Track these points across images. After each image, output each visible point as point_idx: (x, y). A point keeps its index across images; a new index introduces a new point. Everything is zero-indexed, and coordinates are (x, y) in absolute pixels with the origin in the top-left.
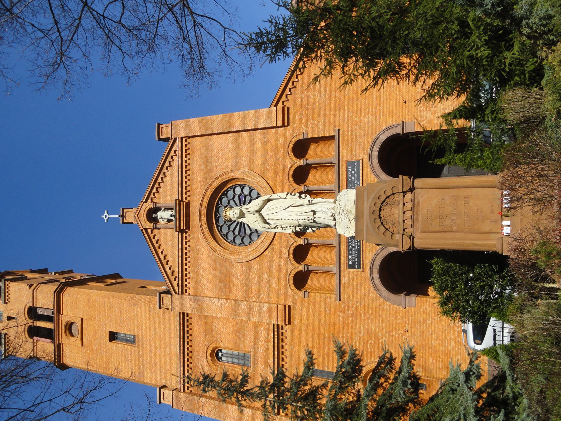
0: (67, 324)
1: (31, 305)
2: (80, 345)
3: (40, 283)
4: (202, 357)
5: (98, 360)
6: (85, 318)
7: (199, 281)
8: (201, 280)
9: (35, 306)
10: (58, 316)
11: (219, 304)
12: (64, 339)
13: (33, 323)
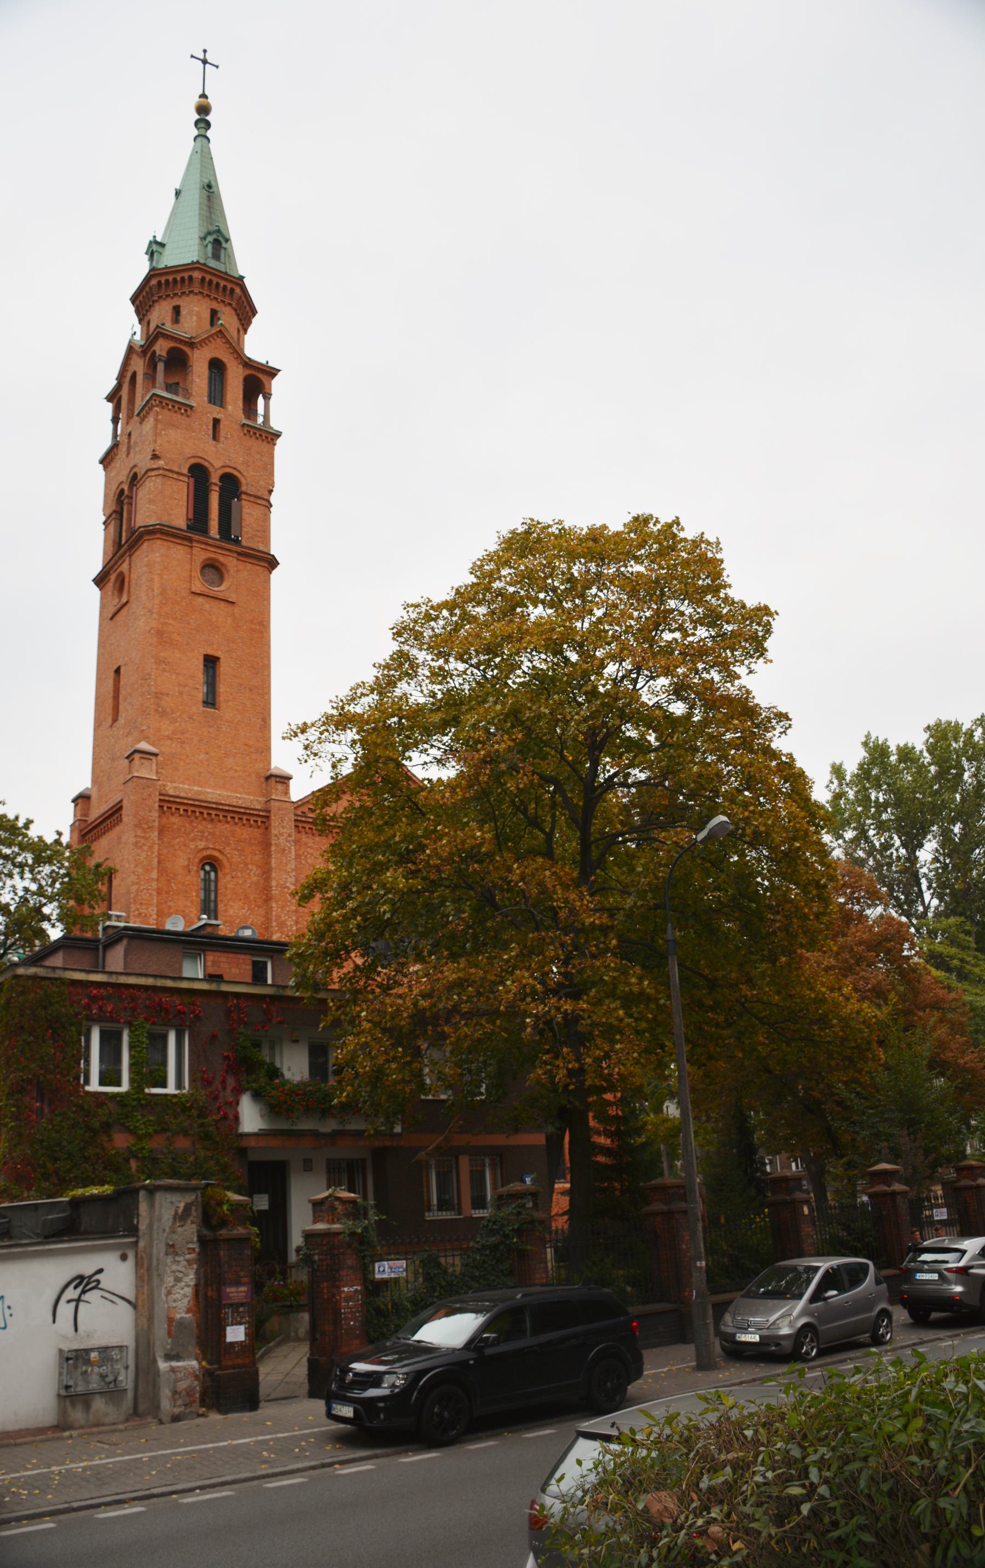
0: (222, 564)
1: (244, 488)
2: (193, 590)
4: (207, 840)
5: (171, 622)
6: (236, 610)
7: (311, 851)
8: (312, 855)
9: (243, 496)
10: (236, 552)
11: (288, 884)
13: (216, 484)
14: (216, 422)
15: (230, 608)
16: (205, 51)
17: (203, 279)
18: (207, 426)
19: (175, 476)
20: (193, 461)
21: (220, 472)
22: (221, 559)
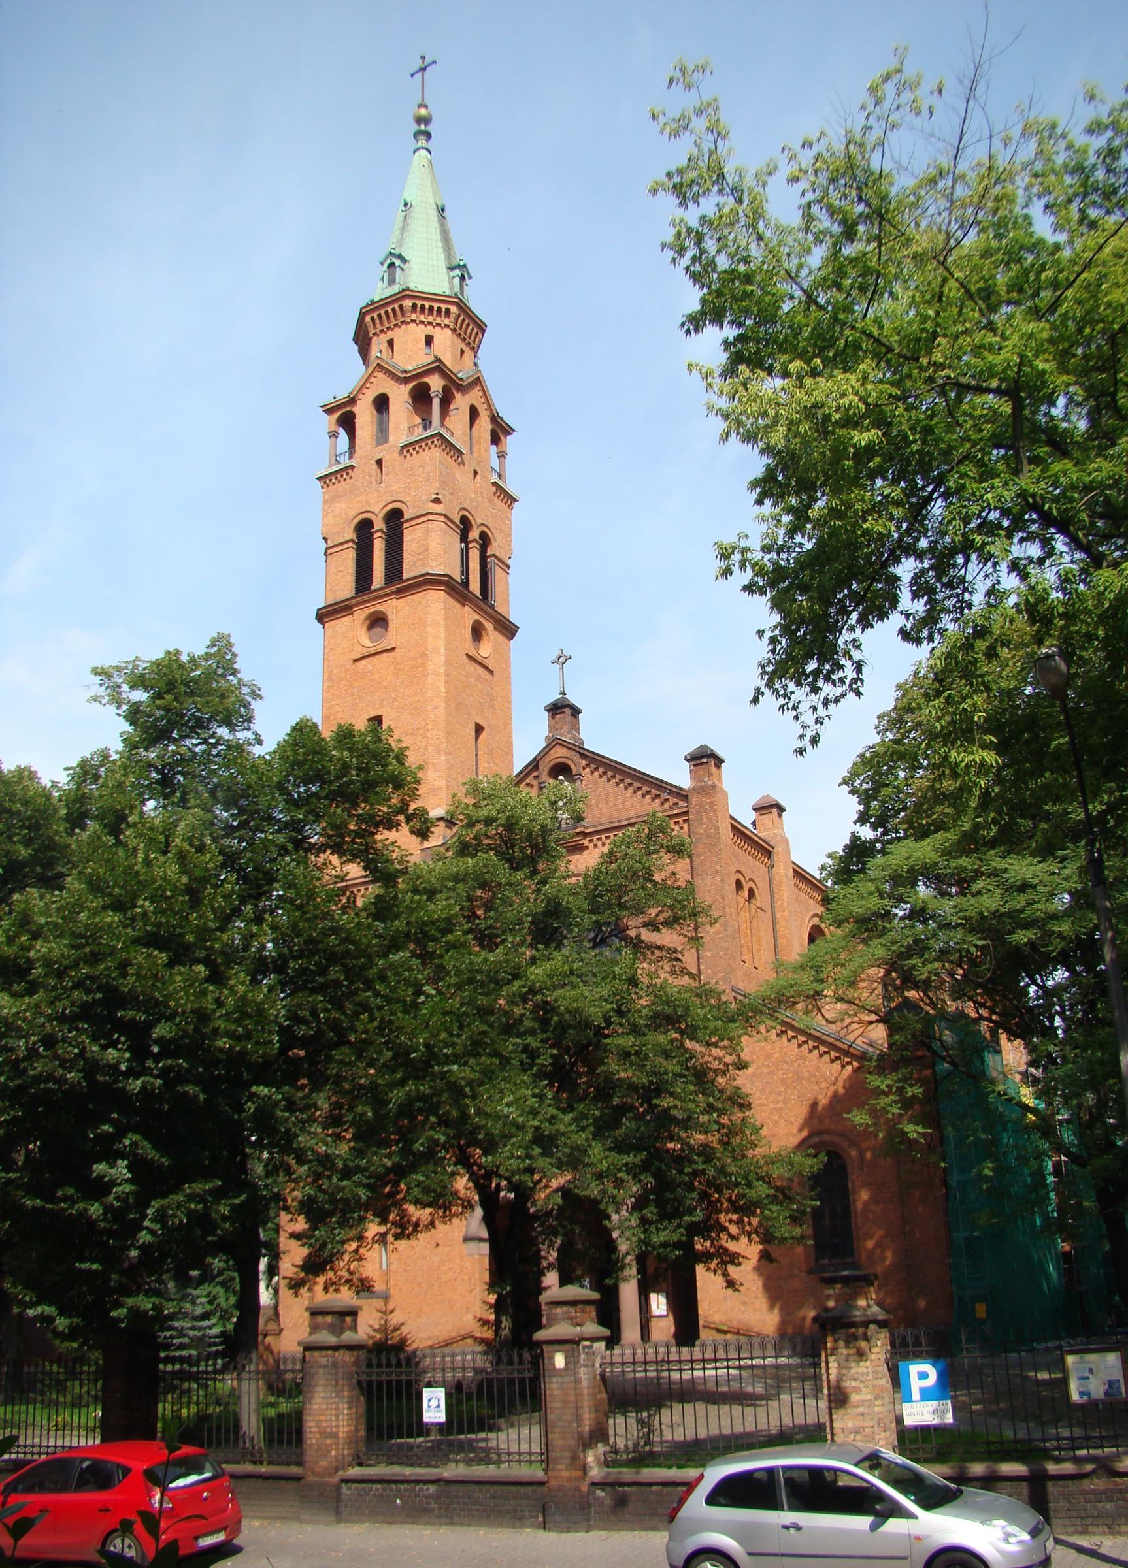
0: (382, 613)
1: (406, 517)
3: (445, 515)
5: (338, 701)
9: (405, 525)
12: (361, 615)
13: (377, 531)
14: (379, 463)
15: (391, 654)
16: (423, 58)
17: (414, 306)
18: (370, 476)
19: (340, 548)
20: (357, 520)
21: (381, 515)
22: (379, 608)
